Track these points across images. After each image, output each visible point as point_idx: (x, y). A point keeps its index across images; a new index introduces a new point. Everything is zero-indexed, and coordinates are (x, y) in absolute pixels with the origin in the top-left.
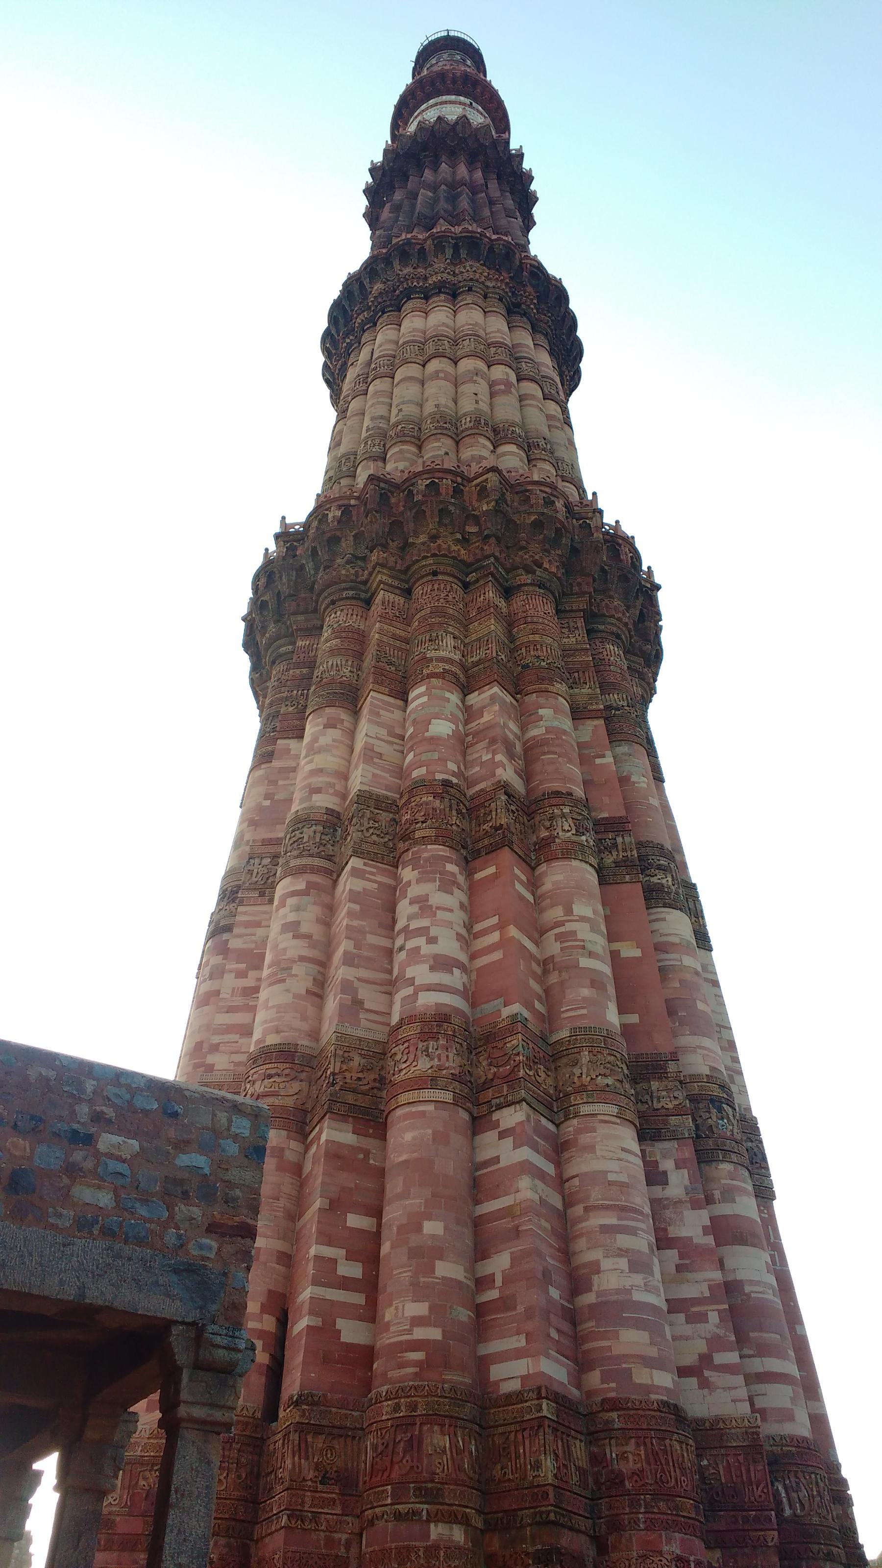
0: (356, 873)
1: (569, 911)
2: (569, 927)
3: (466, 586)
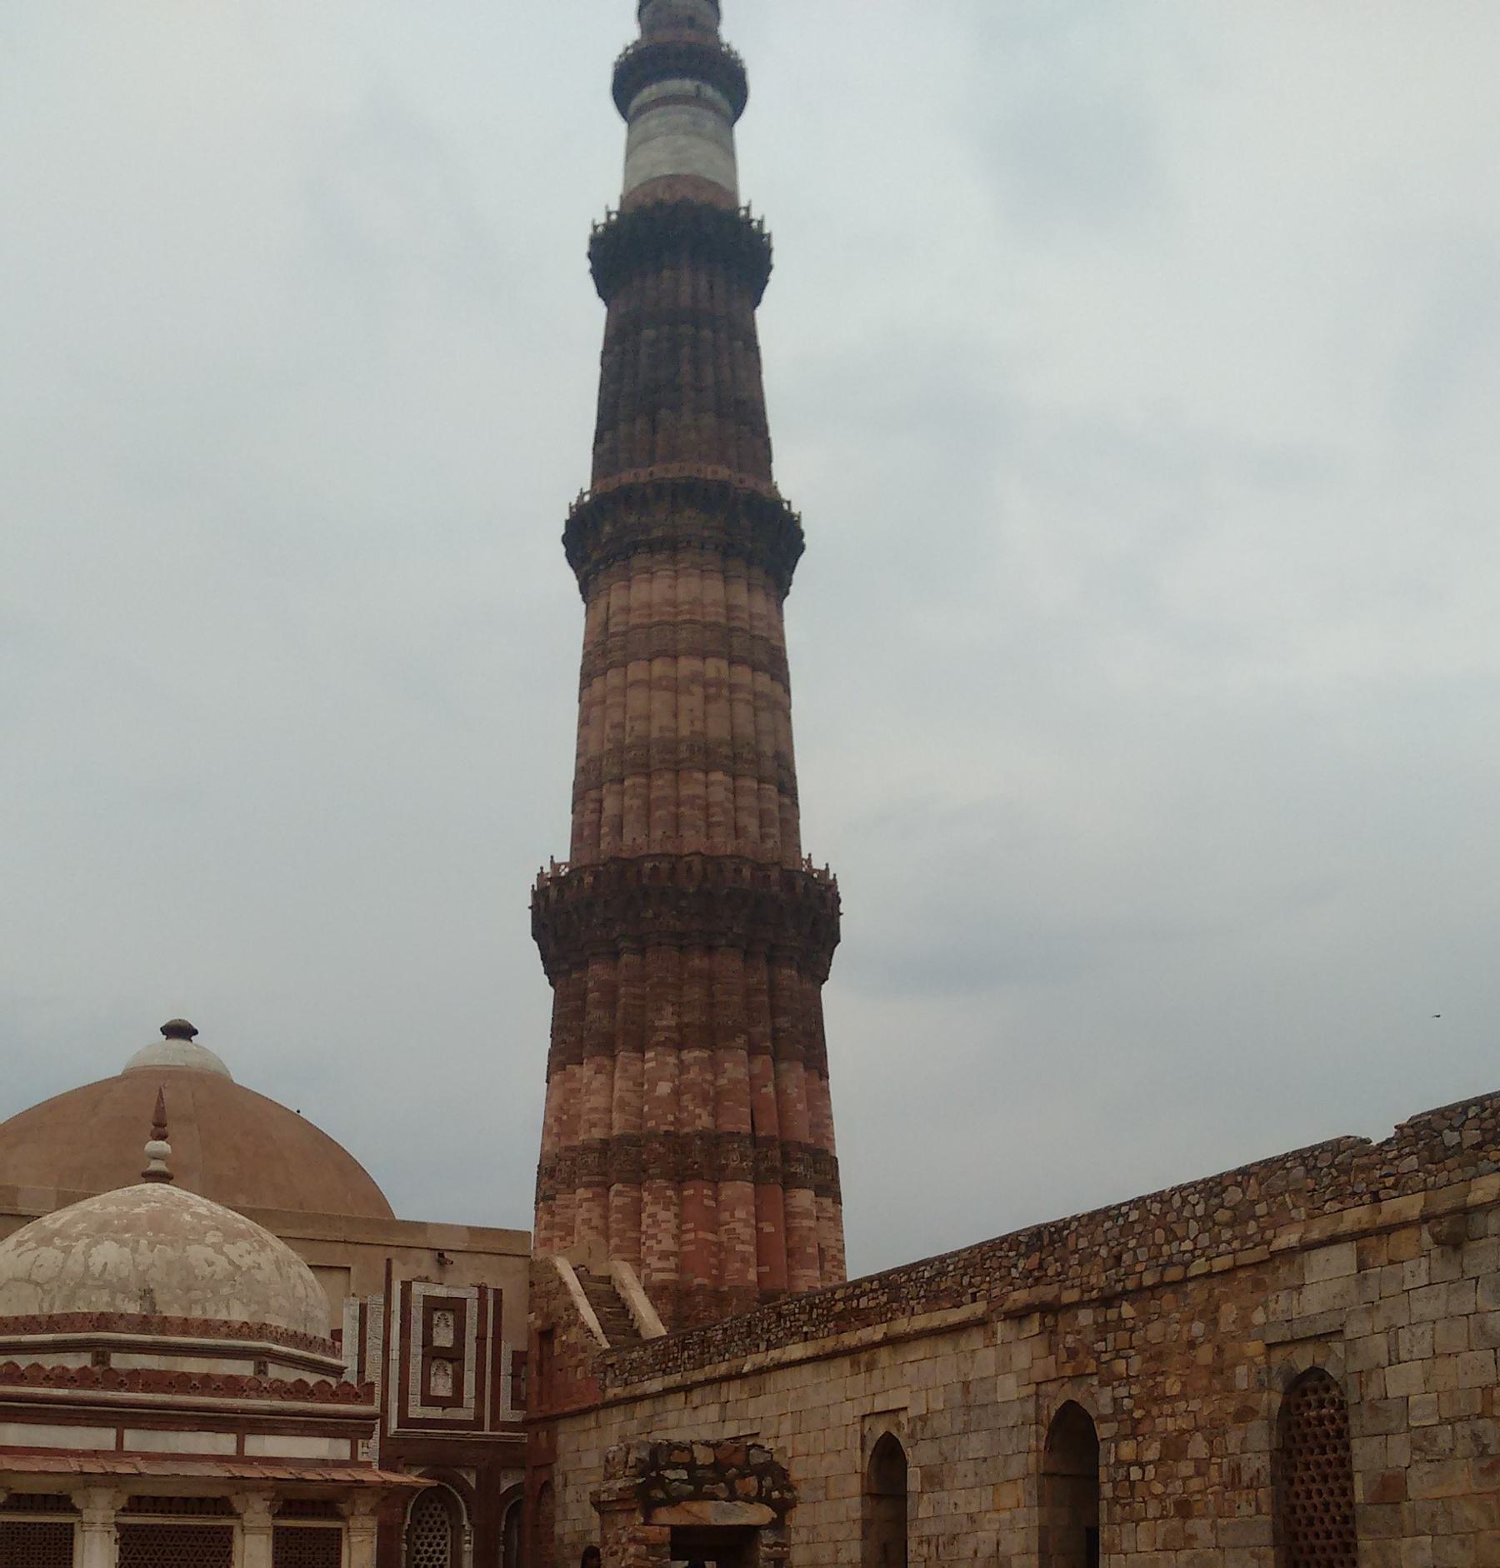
0: (619, 1194)
1: (732, 1215)
2: (731, 1226)
3: (681, 948)
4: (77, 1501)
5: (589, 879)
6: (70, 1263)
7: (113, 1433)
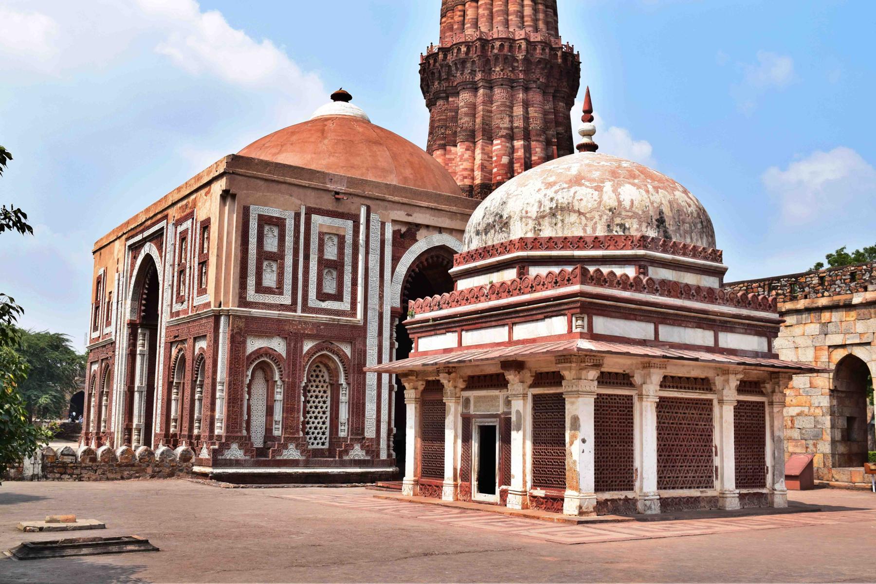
4: (637, 379)
5: (464, 49)
6: (605, 198)
7: (651, 327)
